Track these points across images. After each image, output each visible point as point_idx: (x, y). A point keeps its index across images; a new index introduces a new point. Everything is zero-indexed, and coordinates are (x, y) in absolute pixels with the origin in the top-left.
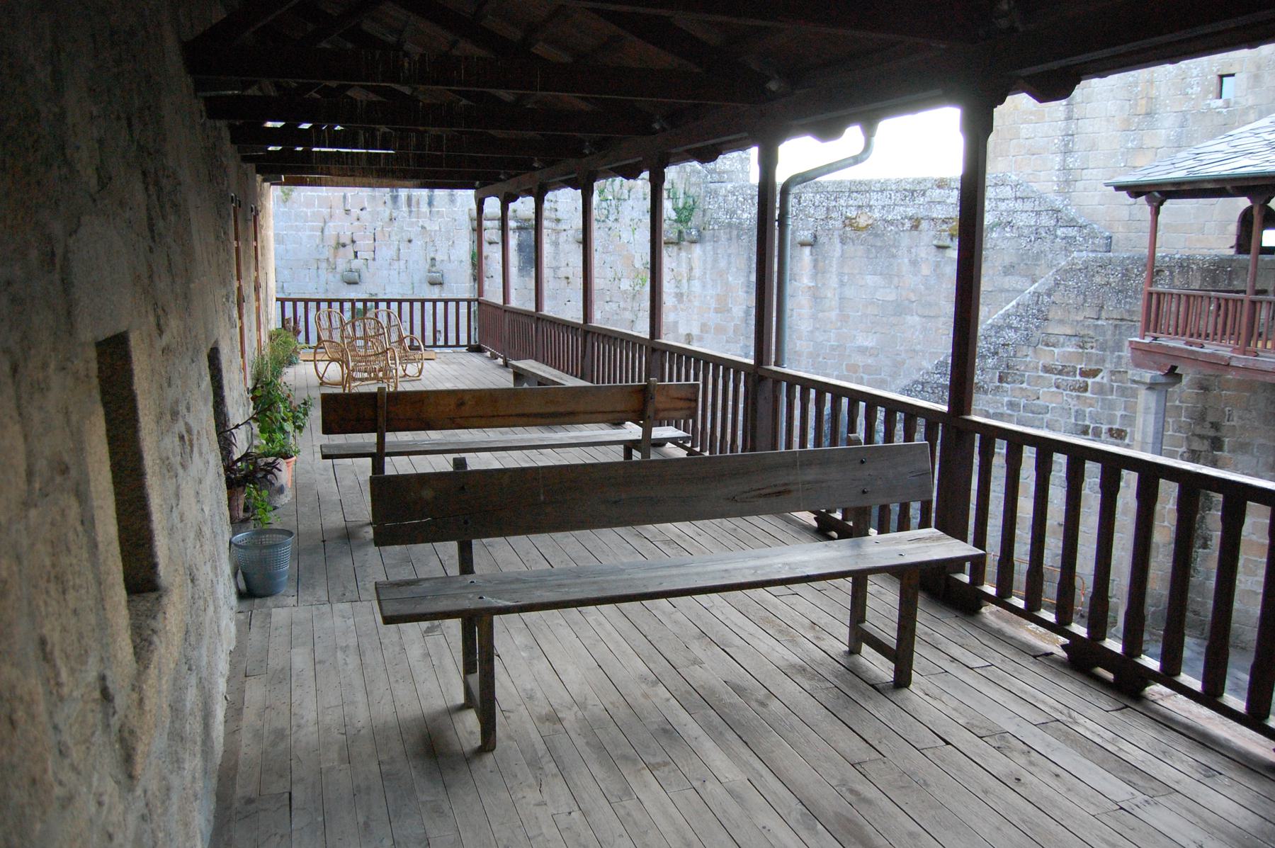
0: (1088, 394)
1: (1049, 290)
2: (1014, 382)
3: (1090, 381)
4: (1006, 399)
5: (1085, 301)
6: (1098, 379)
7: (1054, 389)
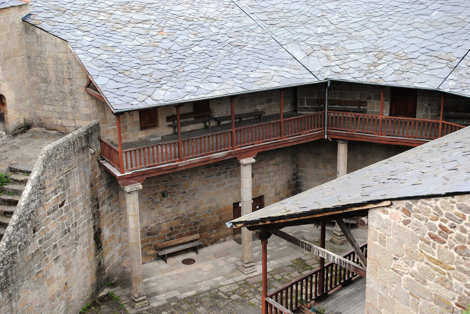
0: (64, 214)
1: (42, 172)
2: (39, 229)
3: (63, 208)
4: (37, 240)
5: (56, 170)
6: (65, 205)
7: (53, 221)
